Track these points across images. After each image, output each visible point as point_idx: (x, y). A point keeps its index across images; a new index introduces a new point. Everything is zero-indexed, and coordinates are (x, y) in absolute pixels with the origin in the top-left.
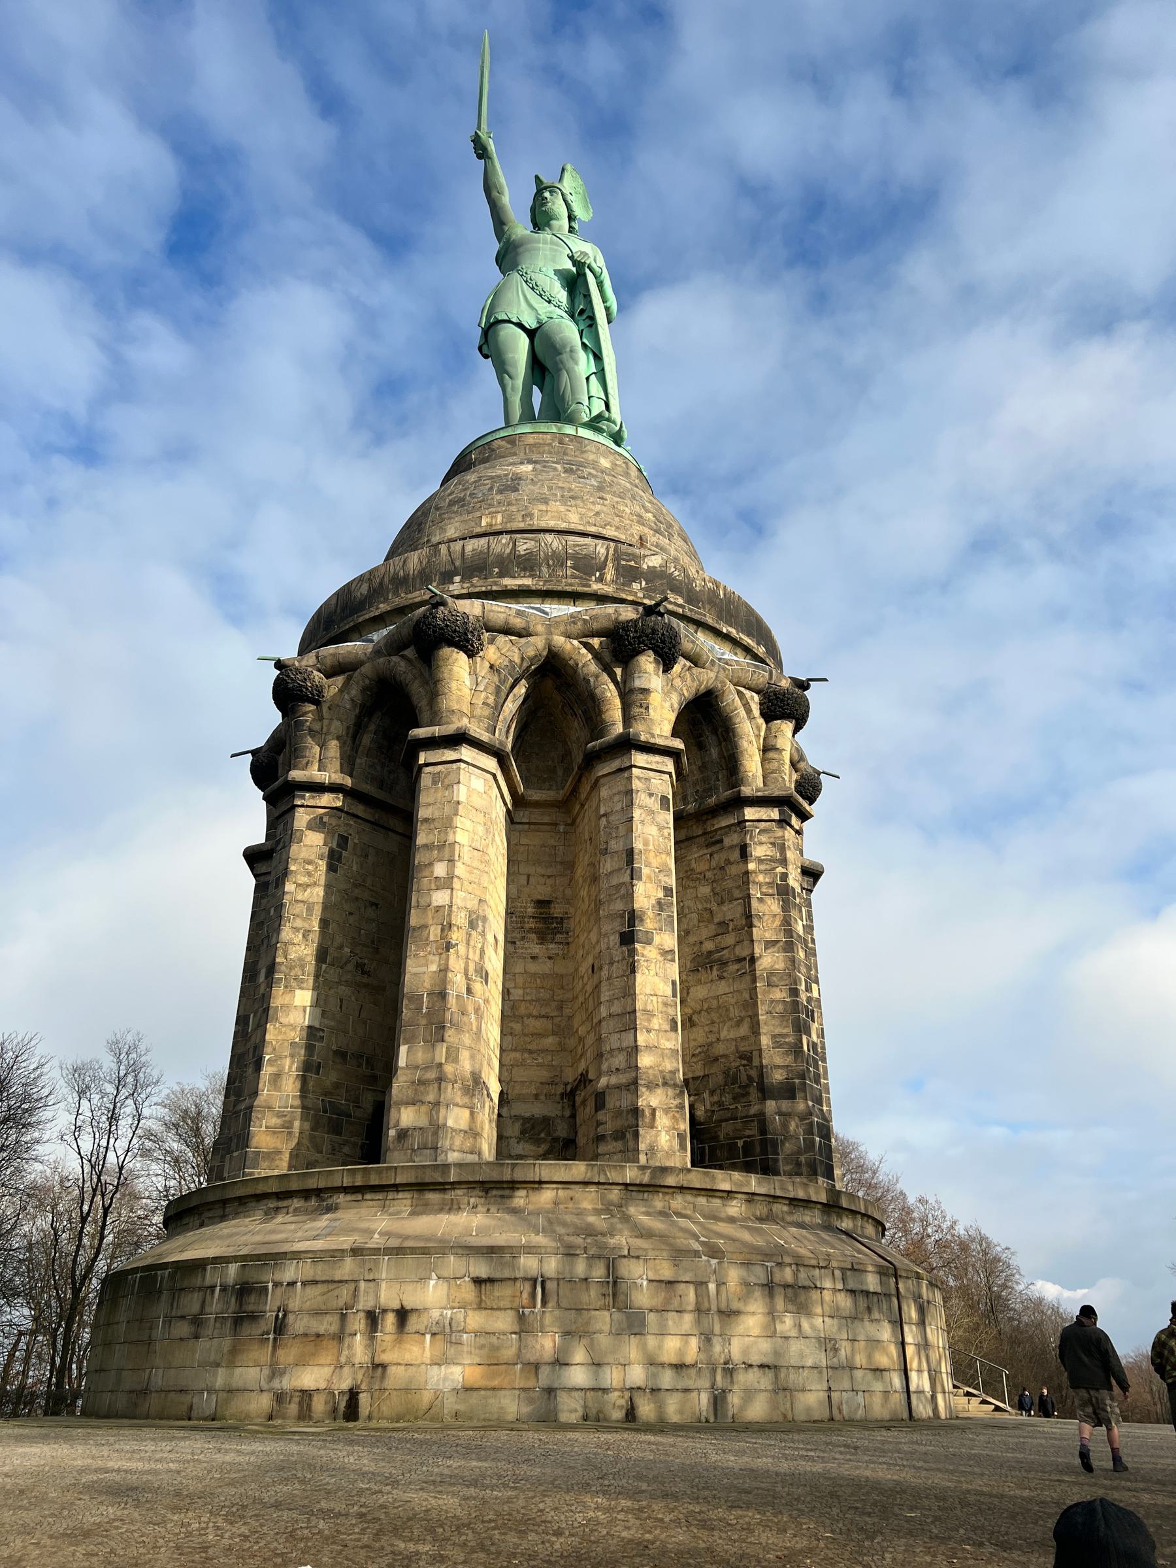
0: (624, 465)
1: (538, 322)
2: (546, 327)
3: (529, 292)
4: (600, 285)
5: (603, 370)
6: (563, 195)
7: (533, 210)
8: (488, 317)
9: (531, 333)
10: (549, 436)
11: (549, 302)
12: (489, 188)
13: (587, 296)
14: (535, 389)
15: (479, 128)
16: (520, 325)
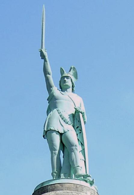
0: (94, 193)
1: (64, 131)
2: (67, 134)
3: (61, 119)
4: (83, 116)
5: (84, 149)
6: (71, 79)
7: (60, 82)
8: (47, 128)
9: (61, 134)
10: (73, 185)
11: (67, 123)
12: (46, 72)
13: (80, 121)
14: (61, 151)
15: (42, 48)
16: (58, 132)
